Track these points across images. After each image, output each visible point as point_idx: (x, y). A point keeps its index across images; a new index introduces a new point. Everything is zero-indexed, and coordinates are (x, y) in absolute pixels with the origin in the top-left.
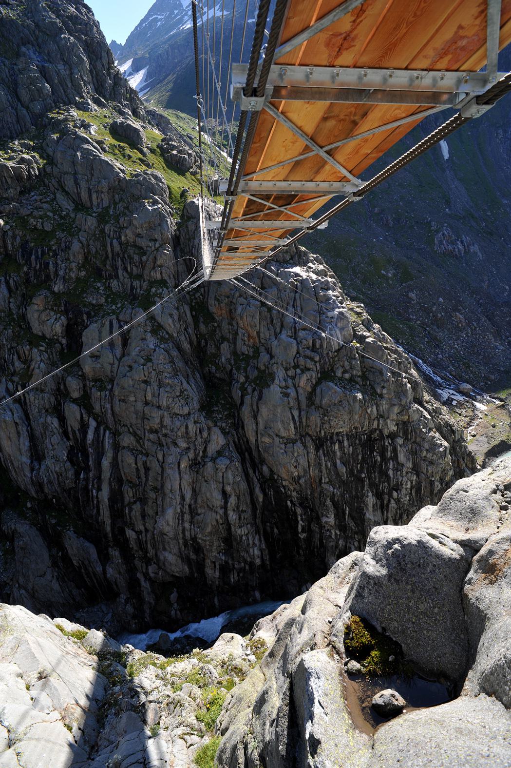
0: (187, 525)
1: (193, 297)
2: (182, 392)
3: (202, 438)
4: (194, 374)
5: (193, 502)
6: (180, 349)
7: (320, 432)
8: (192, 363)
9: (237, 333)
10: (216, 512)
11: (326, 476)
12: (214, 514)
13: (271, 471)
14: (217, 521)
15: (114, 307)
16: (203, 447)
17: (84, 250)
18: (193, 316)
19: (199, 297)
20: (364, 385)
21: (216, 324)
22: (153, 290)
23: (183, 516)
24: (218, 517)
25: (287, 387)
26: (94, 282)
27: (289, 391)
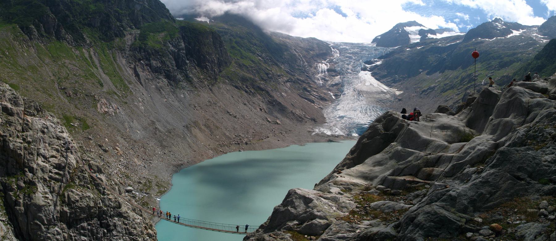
27: (47, 196)
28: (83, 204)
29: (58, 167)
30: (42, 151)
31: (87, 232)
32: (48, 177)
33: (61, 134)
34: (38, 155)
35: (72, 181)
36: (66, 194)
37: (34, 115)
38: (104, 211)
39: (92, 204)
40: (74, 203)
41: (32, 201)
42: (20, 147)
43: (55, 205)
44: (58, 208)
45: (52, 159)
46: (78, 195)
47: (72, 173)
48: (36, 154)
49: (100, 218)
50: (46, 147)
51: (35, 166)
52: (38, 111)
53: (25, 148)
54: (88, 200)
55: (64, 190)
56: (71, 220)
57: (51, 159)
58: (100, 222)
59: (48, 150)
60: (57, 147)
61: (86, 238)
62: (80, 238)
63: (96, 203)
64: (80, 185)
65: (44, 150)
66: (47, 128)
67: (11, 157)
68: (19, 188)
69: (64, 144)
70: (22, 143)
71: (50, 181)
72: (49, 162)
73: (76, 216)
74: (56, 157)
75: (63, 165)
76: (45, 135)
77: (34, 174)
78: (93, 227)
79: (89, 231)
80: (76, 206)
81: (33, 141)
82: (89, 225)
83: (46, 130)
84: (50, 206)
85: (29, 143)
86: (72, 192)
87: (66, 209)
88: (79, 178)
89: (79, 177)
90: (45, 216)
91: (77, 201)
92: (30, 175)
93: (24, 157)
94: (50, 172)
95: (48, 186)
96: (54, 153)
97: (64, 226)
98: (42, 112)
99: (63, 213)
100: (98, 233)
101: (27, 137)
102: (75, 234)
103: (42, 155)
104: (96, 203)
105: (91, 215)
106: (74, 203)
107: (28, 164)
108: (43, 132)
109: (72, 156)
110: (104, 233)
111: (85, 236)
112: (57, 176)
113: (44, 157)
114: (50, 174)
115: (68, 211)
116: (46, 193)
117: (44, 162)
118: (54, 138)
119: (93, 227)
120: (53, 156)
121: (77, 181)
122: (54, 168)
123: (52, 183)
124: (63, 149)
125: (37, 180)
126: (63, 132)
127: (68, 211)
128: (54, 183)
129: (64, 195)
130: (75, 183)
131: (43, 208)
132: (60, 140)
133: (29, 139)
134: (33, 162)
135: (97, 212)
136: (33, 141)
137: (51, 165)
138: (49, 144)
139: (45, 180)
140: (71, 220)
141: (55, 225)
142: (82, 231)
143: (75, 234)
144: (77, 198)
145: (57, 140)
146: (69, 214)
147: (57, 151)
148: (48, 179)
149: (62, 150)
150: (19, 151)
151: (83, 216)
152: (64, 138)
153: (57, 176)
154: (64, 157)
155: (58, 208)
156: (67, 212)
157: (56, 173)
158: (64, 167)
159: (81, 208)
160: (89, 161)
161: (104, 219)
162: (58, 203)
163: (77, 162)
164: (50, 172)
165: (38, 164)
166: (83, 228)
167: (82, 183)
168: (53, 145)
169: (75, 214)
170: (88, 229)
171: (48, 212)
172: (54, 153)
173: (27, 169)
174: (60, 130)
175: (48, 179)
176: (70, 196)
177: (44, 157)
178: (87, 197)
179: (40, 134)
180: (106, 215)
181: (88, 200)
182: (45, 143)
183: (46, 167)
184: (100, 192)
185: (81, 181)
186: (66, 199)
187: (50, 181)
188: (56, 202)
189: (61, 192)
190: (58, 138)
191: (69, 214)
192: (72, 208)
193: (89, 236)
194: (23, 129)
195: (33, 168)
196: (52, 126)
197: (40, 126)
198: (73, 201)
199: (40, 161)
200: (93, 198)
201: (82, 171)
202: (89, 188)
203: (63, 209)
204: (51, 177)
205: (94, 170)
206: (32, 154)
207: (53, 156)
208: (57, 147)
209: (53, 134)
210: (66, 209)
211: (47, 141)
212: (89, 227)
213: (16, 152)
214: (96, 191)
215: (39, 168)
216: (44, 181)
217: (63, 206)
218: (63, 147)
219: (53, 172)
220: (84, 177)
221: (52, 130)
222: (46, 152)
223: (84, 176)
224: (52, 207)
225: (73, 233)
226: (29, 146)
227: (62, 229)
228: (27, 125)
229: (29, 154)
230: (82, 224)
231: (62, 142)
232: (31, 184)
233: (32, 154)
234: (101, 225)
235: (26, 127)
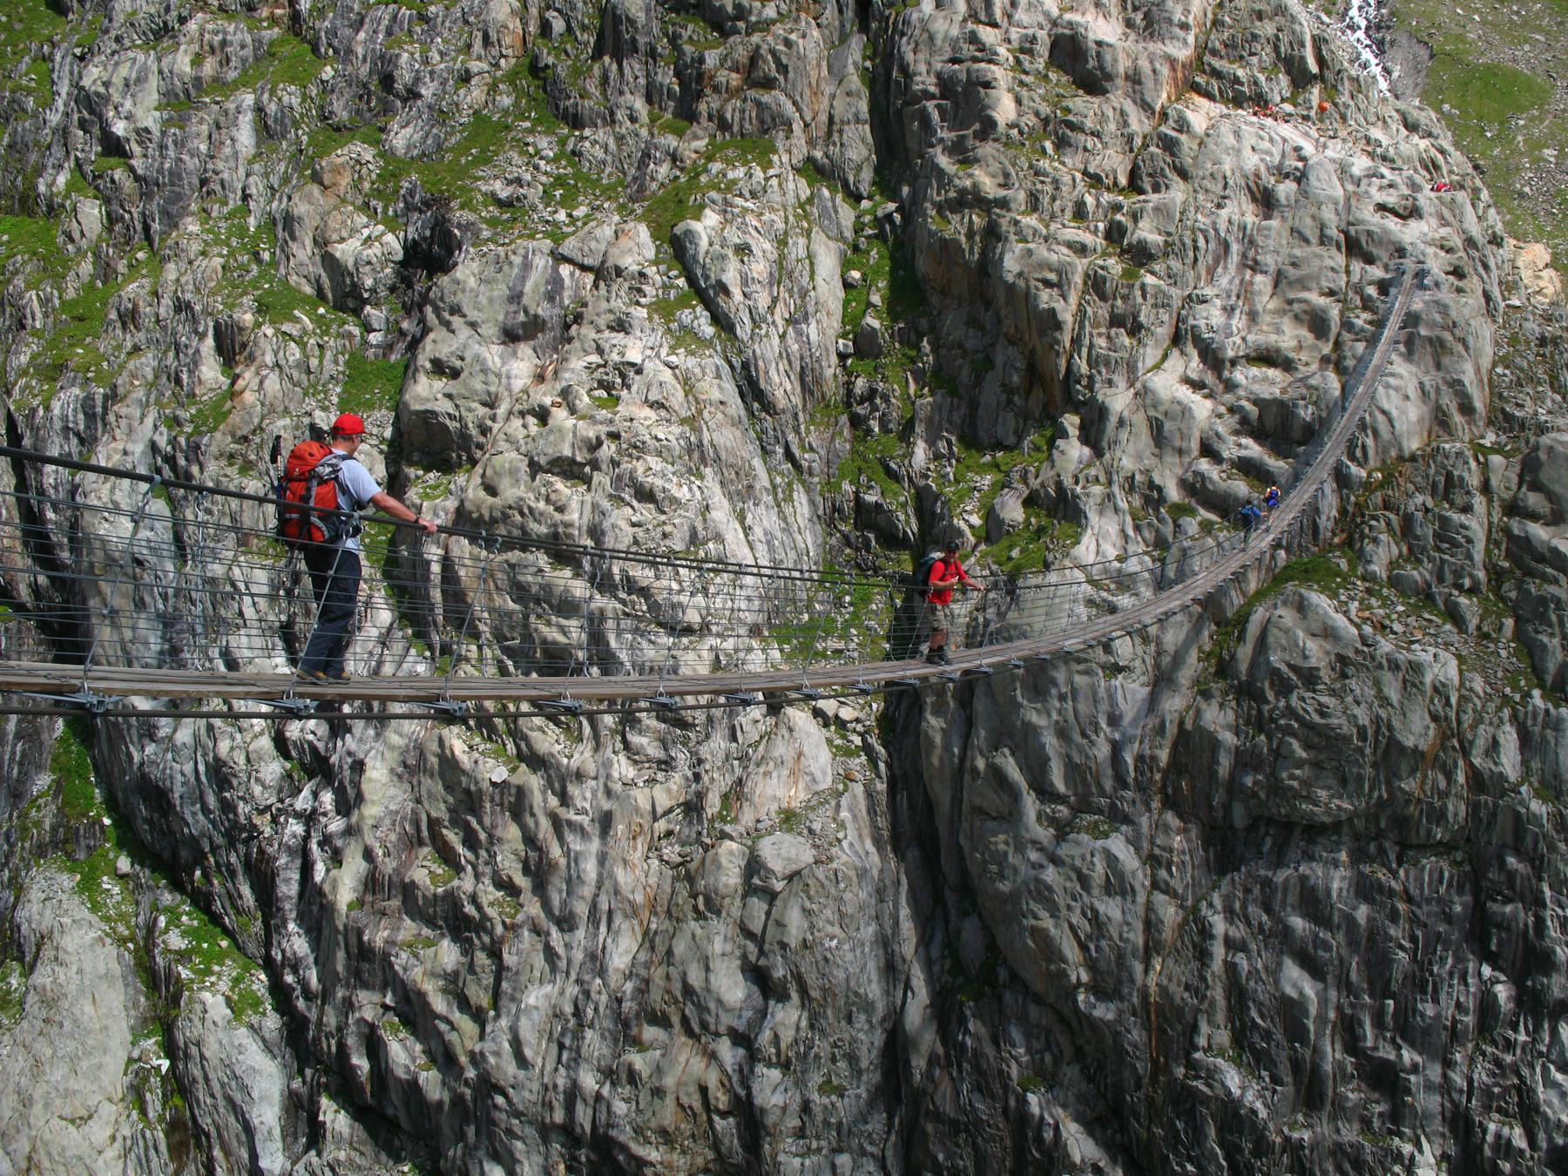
0: (589, 1081)
1: (867, 219)
2: (694, 539)
3: (734, 738)
4: (789, 499)
5: (629, 987)
6: (752, 390)
7: (1227, 807)
8: (789, 455)
9: (989, 362)
10: (712, 1056)
11: (1220, 1017)
12: (698, 1065)
13: (992, 947)
14: (704, 1090)
15: (562, 216)
16: (729, 779)
17: (525, 24)
18: (847, 286)
19: (889, 217)
20: (1486, 636)
21: (924, 323)
22: (716, 167)
23: (578, 1036)
24: (712, 1079)
25: (1124, 582)
26: (531, 131)
28: (1349, 711)
29: (1278, 427)
30: (1210, 317)
31: (1337, 940)
32: (1183, 484)
33: (1392, 223)
34: (1177, 339)
35: (1349, 543)
36: (1258, 616)
37: (1260, 102)
38: (1520, 823)
39: (1417, 731)
40: (1284, 687)
41: (1012, 616)
42: (1062, 271)
43: (1162, 680)
44: (1174, 704)
45: (1254, 371)
46: (1328, 633)
47: (1367, 486)
48: (1164, 332)
49: (1478, 878)
50: (1246, 291)
51: (1119, 400)
52: (1301, 79)
53: (1096, 284)
54: (1393, 693)
55: (1260, 595)
56: (1239, 817)
57: (1239, 375)
58: (1478, 911)
59: (1253, 316)
60: (1322, 301)
61: (1310, 989)
62: (1275, 971)
63: (1453, 737)
64: (1394, 582)
65: (1229, 311)
66: (1301, 178)
67: (1012, 343)
68: (993, 529)
69: (1383, 287)
70: (1081, 250)
71: (1179, 510)
72: (1230, 386)
73: (1276, 788)
74: (1287, 365)
75: (1306, 413)
76: (1274, 223)
77: (1098, 453)
78: (1394, 917)
79: (1352, 943)
80: (1291, 712)
81: (1168, 250)
82: (1365, 890)
83: (1285, 190)
84: (1116, 669)
85: (1140, 256)
86: (1302, 607)
87: (1218, 719)
88: (1407, 528)
89: (1407, 520)
90: (1062, 733)
91: (1310, 678)
92: (1074, 451)
93: (1076, 341)
94: (1208, 451)
95: (1161, 544)
96: (1289, 336)
97: (1177, 841)
98: (1331, 90)
99: (1192, 745)
100: (1420, 982)
101: (1135, 217)
102: (1239, 932)
103: (1198, 341)
104: (1453, 737)
105: (1402, 823)
106: (1284, 688)
107: (1090, 387)
108: (1265, 201)
109: (1400, 366)
110: (1487, 1004)
111: (1314, 968)
112: (1241, 487)
113: (1212, 357)
114: (1204, 465)
115: (1228, 738)
116: (1124, 582)
117: (1197, 386)
118: (1323, 240)
119: (1394, 917)
120: (1266, 358)
121: (1382, 554)
122: (1246, 427)
123: (1191, 525)
124: (1361, 319)
125: (1097, 490)
126: (1411, 213)
127: (1228, 738)
128: (1207, 527)
129: (1242, 619)
130: (1360, 557)
131: (1060, 675)
132: (1369, 260)
133: (1147, 232)
134: (1120, 380)
135: (1457, 810)
136: (1168, 250)
137: (1232, 410)
138: (1279, 279)
139: (1153, 497)
140: (1239, 817)
141: (1118, 818)
142: (1298, 923)
143: (1239, 932)
144: (1316, 653)
145: (1340, 259)
146: (1225, 764)
147: (1317, 323)
148: (1173, 494)
149: (1347, 325)
150: (1046, 298)
151: (1328, 802)
152: (1401, 252)
153: (1241, 487)
154: (1340, 370)
155: (1174, 704)
156: (1214, 744)
157: (1246, 467)
158: (1312, 434)
159: (1323, 740)
160: (1542, 429)
161: (1513, 889)
162: (1185, 676)
163: (1440, 420)
164: (1208, 450)
165: (1144, 395)
166: (1313, 902)
167: (1417, 574)
168: (1302, 284)
169: (1273, 775)
170: (1350, 920)
171: (1083, 707)
172: (1289, 336)
173: (1071, 422)
174: (1391, 199)
175: (1173, 494)
176: (1274, 635)
177: (1212, 357)
178: (1394, 666)
179: (1241, 210)
180: (1538, 865)
181: (1393, 693)
182: (1255, 267)
183: (1185, 412)
184: (1537, 672)
185: (1414, 555)
186: (1245, 653)
187: (1179, 510)
188: (1178, 660)
189: (1236, 599)
190: (1354, 247)
191: (1225, 764)
192: (1260, 723)
193: (1346, 986)
194: (1134, 175)
195: (1102, 412)
196: (1343, 170)
197: (1251, 161)
198: (1275, 672)
199: (1170, 380)
200: (1439, 690)
201: (1449, 487)
202: (1454, 615)
203: (1198, 713)
204: (1196, 489)
205: (1551, 497)
206: (1135, 329)
207: (1266, 358)
208: (1322, 301)
209: (1328, 215)
210: (1218, 719)
211: (1269, 261)
212: (1362, 912)
213: (1028, 297)
214: (1504, 651)
215: (1139, 419)
216: (1147, 500)
217: (1206, 695)
218: (1367, 304)
219: (1229, 450)
220: (1446, 535)
221: (1328, 186)
222: (1238, 322)
223: (1444, 521)
224: (1131, 691)
225: (1229, 913)
226: (1127, 274)
227: (1153, 861)
228: (1169, 145)
229: (1116, 321)
230: (1315, 871)
231: (1376, 272)
232: (1060, 510)
233: (1135, 329)
234: (1480, 934)
235: (1161, 160)
